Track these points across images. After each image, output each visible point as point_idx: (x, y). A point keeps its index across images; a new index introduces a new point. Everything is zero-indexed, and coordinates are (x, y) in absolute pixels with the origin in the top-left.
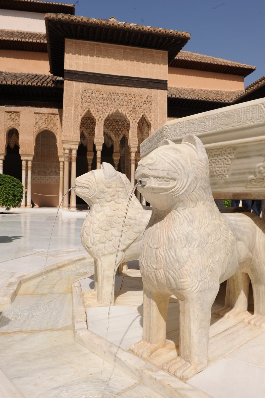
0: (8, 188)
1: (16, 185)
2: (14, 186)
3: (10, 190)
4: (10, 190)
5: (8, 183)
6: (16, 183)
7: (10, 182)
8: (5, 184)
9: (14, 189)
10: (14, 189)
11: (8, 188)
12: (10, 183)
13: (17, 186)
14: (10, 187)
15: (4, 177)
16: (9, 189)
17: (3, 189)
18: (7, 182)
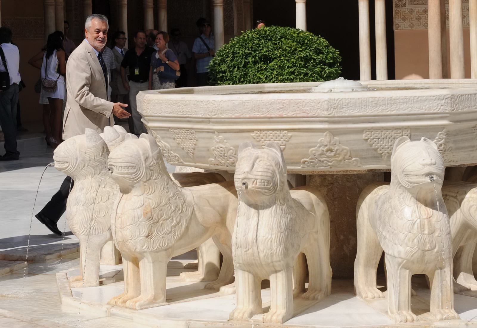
0: (288, 67)
1: (311, 58)
2: (306, 59)
3: (293, 73)
4: (293, 73)
5: (288, 53)
6: (311, 53)
7: (295, 49)
8: (280, 57)
9: (305, 71)
10: (305, 71)
11: (288, 67)
12: (293, 53)
13: (315, 59)
14: (294, 65)
15: (281, 37)
16: (292, 70)
17: (275, 73)
18: (286, 50)
